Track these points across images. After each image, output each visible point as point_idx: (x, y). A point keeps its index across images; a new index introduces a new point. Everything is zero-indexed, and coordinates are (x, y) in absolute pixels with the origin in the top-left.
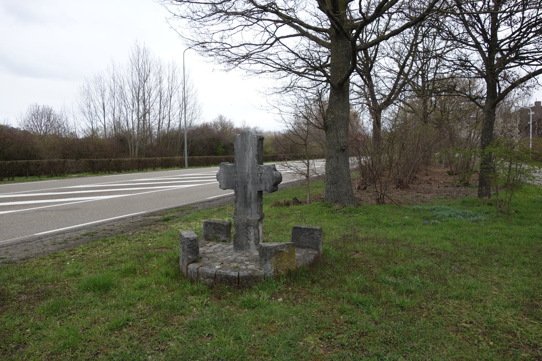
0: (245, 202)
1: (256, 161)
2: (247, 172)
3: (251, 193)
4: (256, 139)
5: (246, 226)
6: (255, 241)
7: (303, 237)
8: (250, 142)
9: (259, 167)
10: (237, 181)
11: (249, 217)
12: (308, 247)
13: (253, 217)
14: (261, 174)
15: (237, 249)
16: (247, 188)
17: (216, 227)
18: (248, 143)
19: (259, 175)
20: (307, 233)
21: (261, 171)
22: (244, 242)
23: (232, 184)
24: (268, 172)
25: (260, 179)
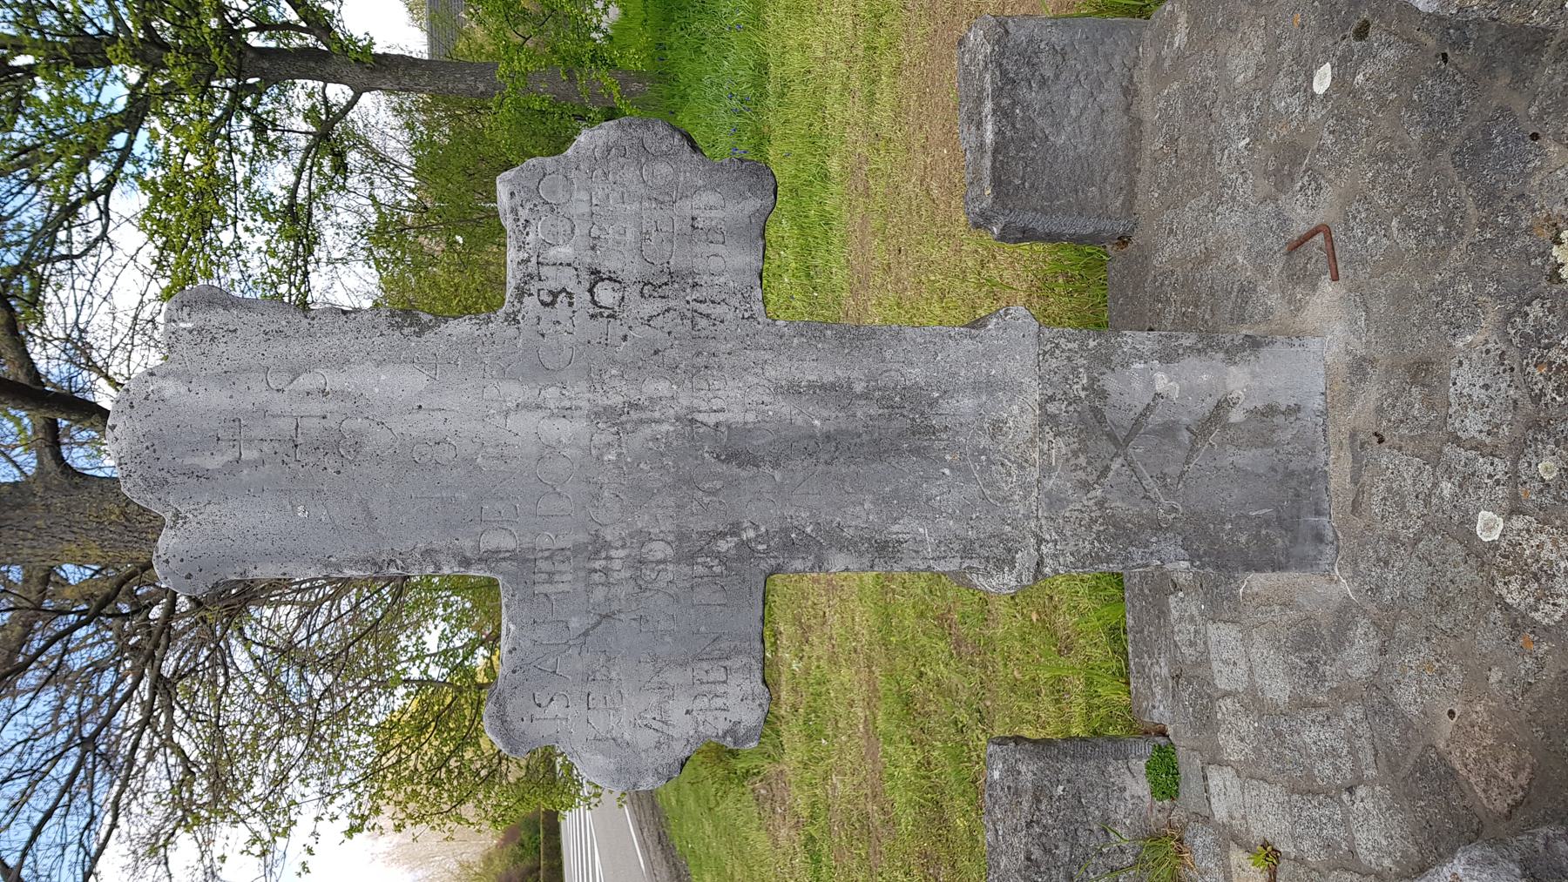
0: (880, 449)
1: (461, 328)
2: (580, 425)
3: (793, 390)
5: (1107, 447)
6: (1231, 355)
7: (1058, 126)
8: (256, 393)
9: (521, 293)
10: (682, 537)
11: (1021, 415)
12: (1129, 91)
14: (597, 276)
15: (1319, 538)
16: (746, 431)
17: (1063, 850)
18: (264, 413)
19: (606, 294)
20: (1033, 96)
21: (566, 278)
22: (1246, 458)
23: (704, 595)
24: (579, 206)
25: (649, 287)
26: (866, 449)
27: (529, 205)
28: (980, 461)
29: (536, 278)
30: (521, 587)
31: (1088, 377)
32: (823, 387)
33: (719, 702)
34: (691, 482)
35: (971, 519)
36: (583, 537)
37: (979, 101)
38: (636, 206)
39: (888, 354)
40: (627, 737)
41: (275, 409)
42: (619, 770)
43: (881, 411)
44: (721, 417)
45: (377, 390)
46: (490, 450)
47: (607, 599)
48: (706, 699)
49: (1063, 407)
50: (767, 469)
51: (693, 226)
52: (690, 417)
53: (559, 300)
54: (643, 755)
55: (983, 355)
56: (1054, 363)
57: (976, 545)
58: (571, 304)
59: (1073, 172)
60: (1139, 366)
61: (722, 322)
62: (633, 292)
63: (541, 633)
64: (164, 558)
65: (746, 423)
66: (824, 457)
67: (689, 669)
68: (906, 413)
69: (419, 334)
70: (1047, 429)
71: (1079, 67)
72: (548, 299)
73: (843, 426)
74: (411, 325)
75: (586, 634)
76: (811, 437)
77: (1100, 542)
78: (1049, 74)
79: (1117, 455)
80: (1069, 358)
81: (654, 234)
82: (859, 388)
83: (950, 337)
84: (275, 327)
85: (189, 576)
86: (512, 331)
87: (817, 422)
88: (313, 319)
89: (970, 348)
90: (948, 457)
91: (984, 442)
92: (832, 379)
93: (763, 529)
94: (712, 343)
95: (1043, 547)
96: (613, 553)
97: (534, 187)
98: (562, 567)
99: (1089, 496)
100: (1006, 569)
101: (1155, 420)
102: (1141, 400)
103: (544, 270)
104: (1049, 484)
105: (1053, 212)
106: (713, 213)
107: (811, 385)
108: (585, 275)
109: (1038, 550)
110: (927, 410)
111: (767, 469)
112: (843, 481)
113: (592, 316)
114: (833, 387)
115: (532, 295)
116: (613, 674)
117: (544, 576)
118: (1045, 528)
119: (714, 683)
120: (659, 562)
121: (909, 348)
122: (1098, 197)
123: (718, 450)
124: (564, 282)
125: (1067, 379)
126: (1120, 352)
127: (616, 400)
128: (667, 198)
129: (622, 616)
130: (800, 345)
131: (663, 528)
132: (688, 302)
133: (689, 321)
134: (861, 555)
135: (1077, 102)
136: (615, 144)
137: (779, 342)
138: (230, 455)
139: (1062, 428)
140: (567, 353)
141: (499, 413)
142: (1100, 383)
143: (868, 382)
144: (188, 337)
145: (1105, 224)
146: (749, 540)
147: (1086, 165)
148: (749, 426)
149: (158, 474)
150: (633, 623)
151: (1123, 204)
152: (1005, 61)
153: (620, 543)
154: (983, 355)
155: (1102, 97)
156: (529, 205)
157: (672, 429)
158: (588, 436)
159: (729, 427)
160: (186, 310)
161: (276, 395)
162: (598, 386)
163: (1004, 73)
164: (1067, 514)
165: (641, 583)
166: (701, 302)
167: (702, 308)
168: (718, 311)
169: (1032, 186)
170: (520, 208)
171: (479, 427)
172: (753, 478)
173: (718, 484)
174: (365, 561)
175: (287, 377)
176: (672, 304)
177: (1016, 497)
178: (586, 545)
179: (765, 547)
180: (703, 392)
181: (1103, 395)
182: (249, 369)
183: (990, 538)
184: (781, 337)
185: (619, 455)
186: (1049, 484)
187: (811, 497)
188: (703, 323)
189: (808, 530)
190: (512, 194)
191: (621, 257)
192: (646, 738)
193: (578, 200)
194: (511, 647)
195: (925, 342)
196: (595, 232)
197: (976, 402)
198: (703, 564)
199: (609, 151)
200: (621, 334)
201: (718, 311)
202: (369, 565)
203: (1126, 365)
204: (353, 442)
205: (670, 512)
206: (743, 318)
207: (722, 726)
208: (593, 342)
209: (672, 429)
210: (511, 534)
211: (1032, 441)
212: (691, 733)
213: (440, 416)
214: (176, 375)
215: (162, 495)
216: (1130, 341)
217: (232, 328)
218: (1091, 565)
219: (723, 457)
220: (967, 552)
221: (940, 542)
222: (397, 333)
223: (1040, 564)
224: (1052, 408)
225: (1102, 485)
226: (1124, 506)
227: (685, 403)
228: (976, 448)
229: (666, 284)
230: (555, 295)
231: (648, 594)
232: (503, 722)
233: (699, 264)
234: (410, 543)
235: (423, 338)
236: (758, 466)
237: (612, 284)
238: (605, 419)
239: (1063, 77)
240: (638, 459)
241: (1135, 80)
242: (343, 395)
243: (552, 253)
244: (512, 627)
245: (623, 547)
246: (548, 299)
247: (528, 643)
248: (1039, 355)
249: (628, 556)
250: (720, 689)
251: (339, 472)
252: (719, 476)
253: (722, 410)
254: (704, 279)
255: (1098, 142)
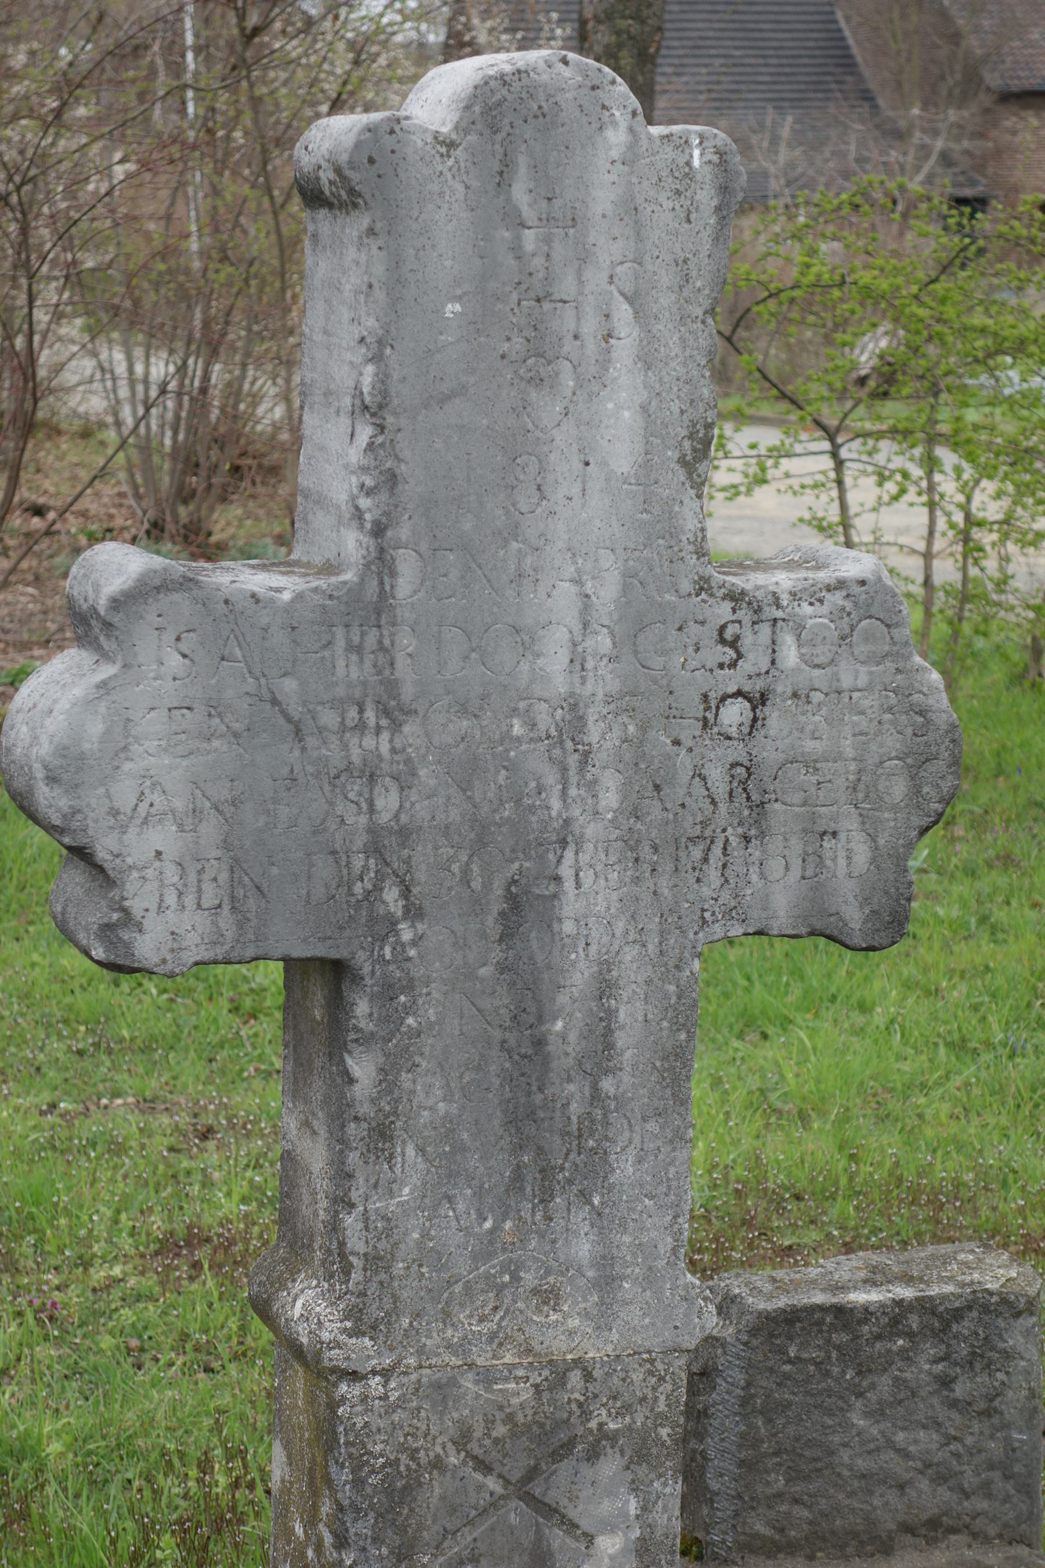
2: (560, 683)
4: (706, 197)
7: (877, 1413)
10: (404, 834)
13: (632, 1315)
14: (758, 701)
16: (549, 921)
18: (584, 257)
19: (734, 713)
21: (755, 660)
23: (324, 869)
26: (523, 1100)
27: (848, 605)
28: (502, 1273)
29: (755, 618)
30: (343, 608)
31: (617, 1430)
32: (608, 1032)
33: (171, 899)
34: (481, 843)
35: (420, 1266)
36: (408, 692)
37: (908, 1280)
38: (850, 753)
39: (652, 1126)
40: (127, 766)
41: (588, 273)
42: (82, 757)
43: (574, 1119)
44: (569, 884)
45: (610, 406)
46: (529, 560)
47: (321, 730)
48: (176, 879)
49: (577, 1395)
50: (496, 954)
51: (825, 833)
52: (569, 839)
53: (727, 649)
54: (101, 791)
55: (650, 1268)
56: (637, 1376)
57: (383, 1276)
58: (721, 666)
59: (810, 1444)
60: (633, 1507)
61: (698, 880)
62: (737, 752)
63: (279, 638)
64: (397, 129)
65: (560, 920)
66: (512, 1038)
67: (218, 853)
68: (572, 1156)
69: (682, 461)
70: (546, 1373)
71: (969, 1440)
72: (728, 634)
73: (555, 1064)
74: (694, 450)
75: (275, 702)
76: (540, 1019)
77: (384, 1466)
78: (960, 1390)
79: (507, 1482)
80: (644, 1399)
81: (814, 779)
82: (607, 1085)
83: (676, 1217)
84: (694, 273)
85: (371, 161)
86: (686, 585)
87: (559, 1025)
88: (703, 322)
89: (660, 1247)
90: (508, 1225)
91: (529, 1278)
92: (620, 1044)
93: (412, 953)
94: (670, 867)
95: (378, 1379)
96: (385, 736)
97: (874, 611)
98: (368, 664)
99: (449, 1445)
100: (348, 1324)
101: (557, 1537)
102: (584, 1515)
103: (765, 629)
104: (468, 1382)
105: (745, 1417)
106: (842, 862)
107: (611, 1014)
108: (760, 684)
109: (374, 1372)
110: (575, 1189)
111: (496, 954)
112: (478, 1068)
113: (705, 697)
114: (609, 1046)
115: (734, 610)
116: (216, 743)
117: (356, 639)
118: (405, 1380)
119: (200, 890)
120: (371, 803)
121: (661, 1157)
122: (769, 1491)
123: (524, 881)
124: (751, 656)
125: (615, 1398)
126: (652, 1476)
127: (594, 733)
128: (861, 796)
129: (297, 753)
130: (666, 996)
131: (418, 806)
132: (724, 830)
133: (698, 833)
134: (373, 1101)
135: (916, 1441)
136: (928, 722)
137: (671, 963)
138: (528, 214)
139: (546, 1396)
140: (658, 662)
141: (578, 571)
142: (609, 1451)
143: (616, 1098)
144: (681, 160)
145: (725, 1508)
146: (397, 933)
147: (819, 1465)
148: (556, 926)
149: (506, 121)
150: (287, 769)
151: (756, 1536)
152: (975, 1314)
153: (398, 746)
154: (650, 1268)
155: (924, 1484)
156: (848, 605)
157: (554, 813)
158: (546, 695)
159: (555, 896)
160: (715, 158)
161: (605, 275)
162: (613, 706)
163: (958, 1315)
164: (423, 1414)
165: (343, 779)
166: (725, 849)
167: (717, 850)
168: (713, 875)
169: (787, 1376)
170: (844, 593)
171: (560, 544)
172: (483, 935)
173: (477, 884)
174: (385, 394)
175: (629, 288)
176: (723, 808)
177: (449, 1332)
178: (396, 697)
179: (388, 957)
180: (603, 857)
181: (593, 1455)
182: (639, 237)
183: (393, 1296)
184: (677, 967)
185: (518, 739)
186: (468, 1382)
187: (456, 1021)
188: (697, 853)
189: (410, 1021)
190: (863, 583)
191: (785, 732)
192: (125, 793)
193: (857, 671)
194: (261, 596)
195: (668, 1180)
196: (817, 697)
197: (585, 1262)
198: (366, 868)
199: (921, 713)
200: (682, 738)
201: (713, 875)
202: (379, 399)
203: (635, 1487)
204: (543, 375)
205: (440, 816)
206: (703, 910)
207: (136, 906)
208: (672, 698)
209: (554, 813)
210: (415, 592)
211: (529, 1351)
212: (129, 860)
213: (575, 490)
214: (633, 146)
215: (479, 126)
216: (668, 1490)
217: (693, 217)
218: (350, 1455)
219: (513, 889)
220: (375, 1262)
221: (389, 1220)
222: (684, 432)
223: (354, 1376)
224: (575, 1378)
225: (464, 1463)
226: (434, 1500)
227: (589, 832)
228: (520, 1266)
229: (748, 798)
230: (734, 643)
231: (327, 788)
232: (158, 589)
233: (775, 844)
234: (406, 454)
235: (677, 467)
236: (501, 940)
237: (748, 723)
238: (568, 717)
239: (955, 1415)
240: (512, 767)
241: (953, 1538)
242: (605, 362)
243: (788, 639)
244: (286, 596)
245: (393, 751)
246: (728, 634)
247: (265, 620)
248: (649, 1352)
249: (380, 757)
250: (190, 900)
251: (503, 357)
252: (487, 886)
253: (578, 885)
254: (755, 851)
255: (856, 1484)
